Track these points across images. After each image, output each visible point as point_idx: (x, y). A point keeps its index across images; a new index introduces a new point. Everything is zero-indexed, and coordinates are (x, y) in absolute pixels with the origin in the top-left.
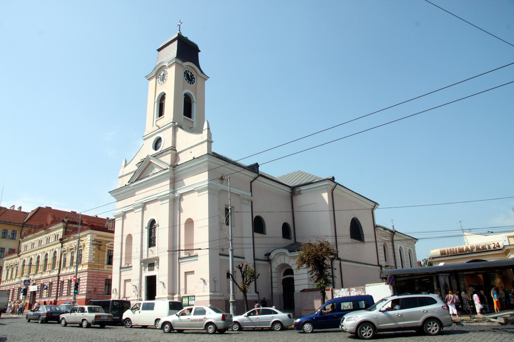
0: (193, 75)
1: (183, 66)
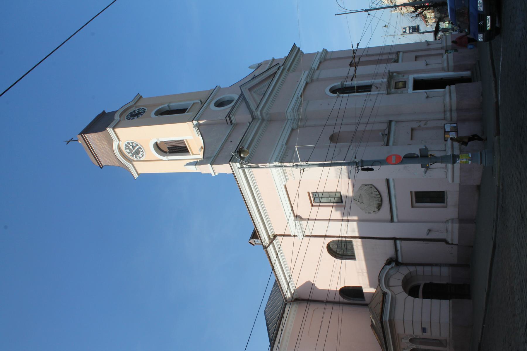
0: (133, 111)
1: (120, 121)
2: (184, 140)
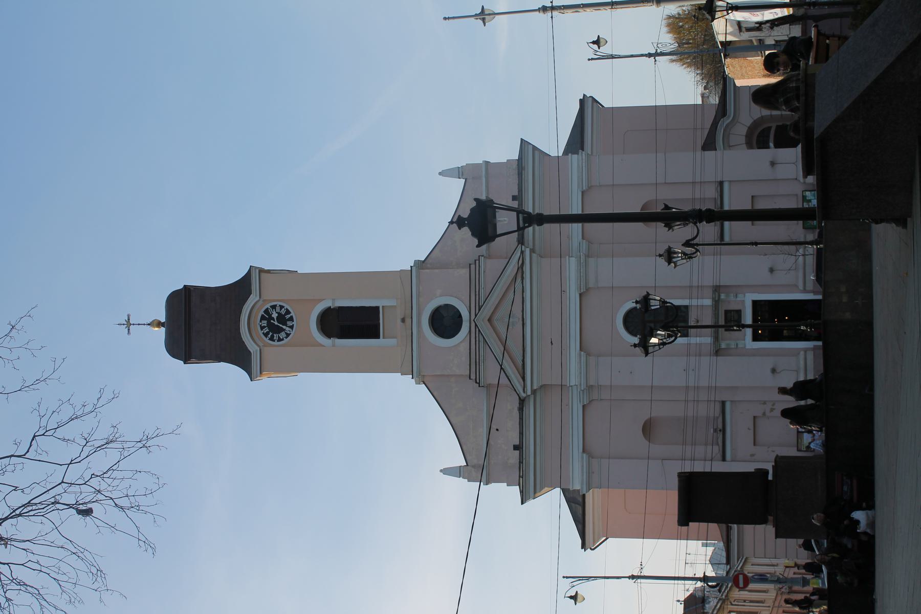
2: (378, 308)
